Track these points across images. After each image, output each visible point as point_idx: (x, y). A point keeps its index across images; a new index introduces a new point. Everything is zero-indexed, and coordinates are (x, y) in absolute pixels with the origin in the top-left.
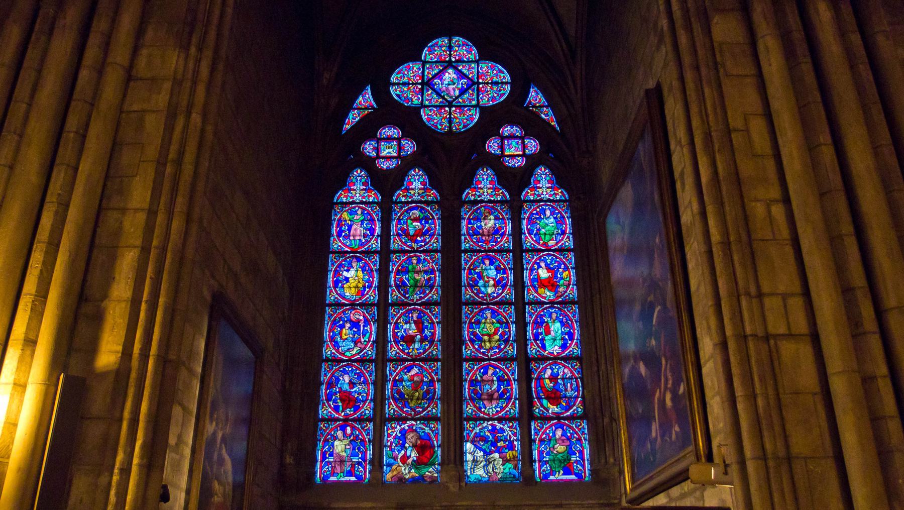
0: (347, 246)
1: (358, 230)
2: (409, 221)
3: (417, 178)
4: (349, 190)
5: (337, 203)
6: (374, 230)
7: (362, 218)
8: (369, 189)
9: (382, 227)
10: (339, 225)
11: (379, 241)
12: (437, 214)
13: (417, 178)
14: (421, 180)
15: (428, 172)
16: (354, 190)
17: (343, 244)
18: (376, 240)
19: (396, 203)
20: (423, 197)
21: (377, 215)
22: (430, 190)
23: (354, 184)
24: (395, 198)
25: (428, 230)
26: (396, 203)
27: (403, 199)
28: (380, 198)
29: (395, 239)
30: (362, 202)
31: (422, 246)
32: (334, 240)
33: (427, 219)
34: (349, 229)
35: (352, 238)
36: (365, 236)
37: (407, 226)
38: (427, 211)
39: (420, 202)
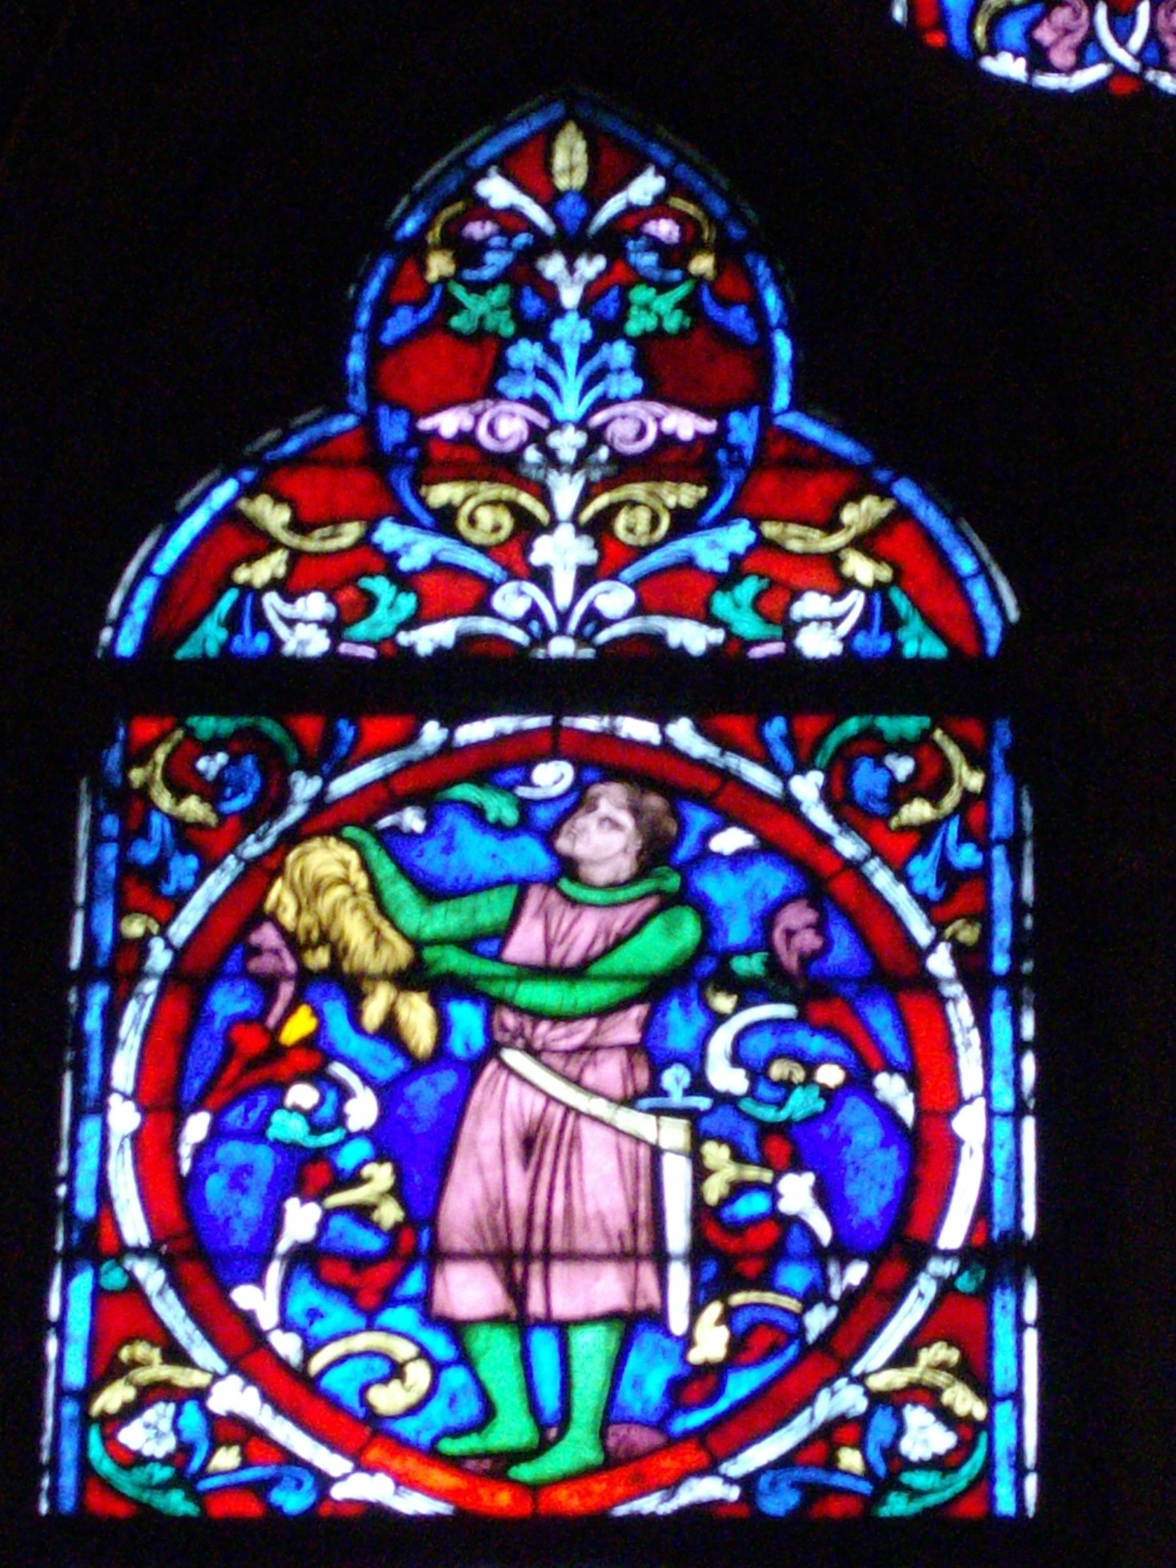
0: (364, 1434)
1: (591, 1144)
4: (392, 475)
5: (165, 683)
6: (924, 1152)
7: (667, 942)
8: (783, 455)
9: (1058, 1107)
10: (221, 1064)
11: (1019, 1357)
16: (473, 460)
17: (297, 1392)
18: (960, 1322)
21: (956, 896)
23: (481, 371)
28: (995, 605)
30: (638, 674)
32: (123, 1317)
34: (421, 1150)
35: (469, 1290)
36: (731, 1252)
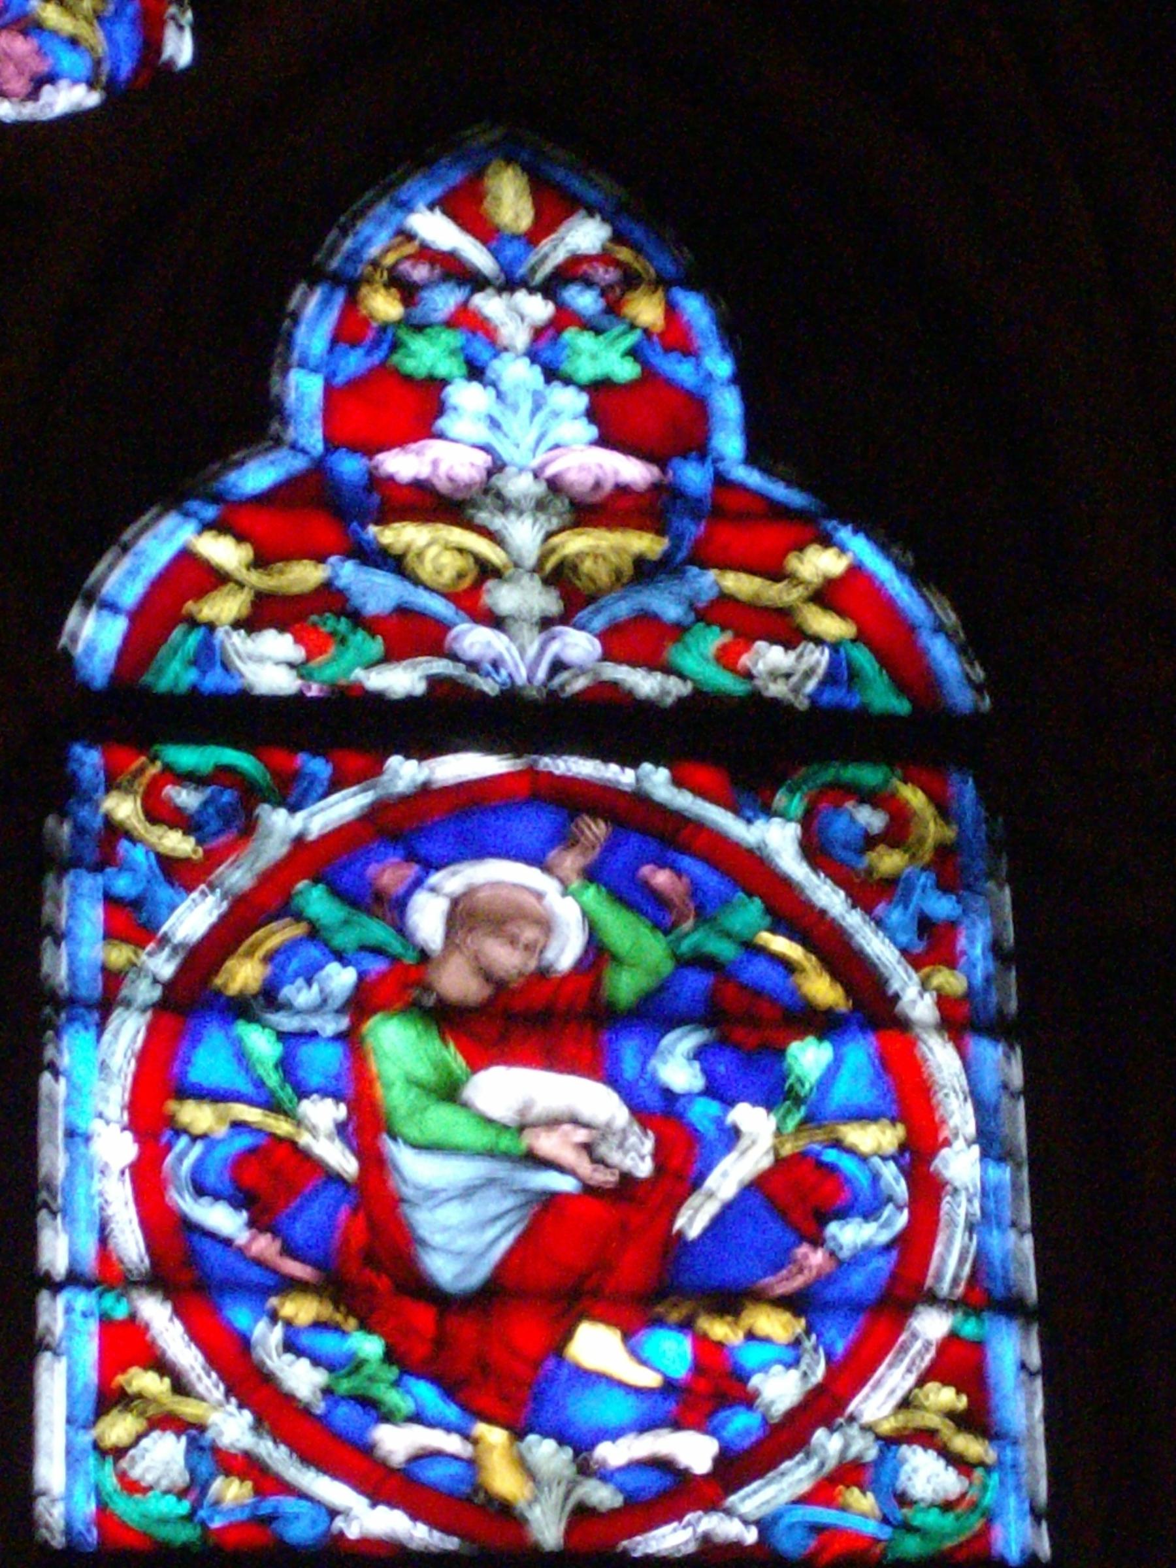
2: (400, 1048)
3: (516, 315)
12: (932, 945)
13: (516, 315)
14: (603, 357)
15: (692, 210)
19: (136, 715)
20: (640, 640)
22: (746, 531)
24: (96, 637)
25: (801, 1194)
26: (136, 715)
27: (269, 664)
29: (125, 1344)
31: (674, 1492)
33: (748, 1030)
37: (366, 1126)
38: (752, 872)
39: (607, 722)
